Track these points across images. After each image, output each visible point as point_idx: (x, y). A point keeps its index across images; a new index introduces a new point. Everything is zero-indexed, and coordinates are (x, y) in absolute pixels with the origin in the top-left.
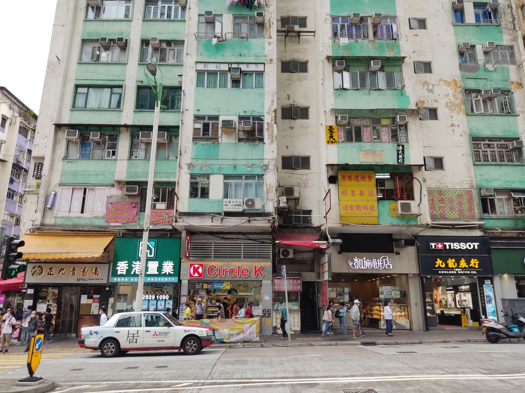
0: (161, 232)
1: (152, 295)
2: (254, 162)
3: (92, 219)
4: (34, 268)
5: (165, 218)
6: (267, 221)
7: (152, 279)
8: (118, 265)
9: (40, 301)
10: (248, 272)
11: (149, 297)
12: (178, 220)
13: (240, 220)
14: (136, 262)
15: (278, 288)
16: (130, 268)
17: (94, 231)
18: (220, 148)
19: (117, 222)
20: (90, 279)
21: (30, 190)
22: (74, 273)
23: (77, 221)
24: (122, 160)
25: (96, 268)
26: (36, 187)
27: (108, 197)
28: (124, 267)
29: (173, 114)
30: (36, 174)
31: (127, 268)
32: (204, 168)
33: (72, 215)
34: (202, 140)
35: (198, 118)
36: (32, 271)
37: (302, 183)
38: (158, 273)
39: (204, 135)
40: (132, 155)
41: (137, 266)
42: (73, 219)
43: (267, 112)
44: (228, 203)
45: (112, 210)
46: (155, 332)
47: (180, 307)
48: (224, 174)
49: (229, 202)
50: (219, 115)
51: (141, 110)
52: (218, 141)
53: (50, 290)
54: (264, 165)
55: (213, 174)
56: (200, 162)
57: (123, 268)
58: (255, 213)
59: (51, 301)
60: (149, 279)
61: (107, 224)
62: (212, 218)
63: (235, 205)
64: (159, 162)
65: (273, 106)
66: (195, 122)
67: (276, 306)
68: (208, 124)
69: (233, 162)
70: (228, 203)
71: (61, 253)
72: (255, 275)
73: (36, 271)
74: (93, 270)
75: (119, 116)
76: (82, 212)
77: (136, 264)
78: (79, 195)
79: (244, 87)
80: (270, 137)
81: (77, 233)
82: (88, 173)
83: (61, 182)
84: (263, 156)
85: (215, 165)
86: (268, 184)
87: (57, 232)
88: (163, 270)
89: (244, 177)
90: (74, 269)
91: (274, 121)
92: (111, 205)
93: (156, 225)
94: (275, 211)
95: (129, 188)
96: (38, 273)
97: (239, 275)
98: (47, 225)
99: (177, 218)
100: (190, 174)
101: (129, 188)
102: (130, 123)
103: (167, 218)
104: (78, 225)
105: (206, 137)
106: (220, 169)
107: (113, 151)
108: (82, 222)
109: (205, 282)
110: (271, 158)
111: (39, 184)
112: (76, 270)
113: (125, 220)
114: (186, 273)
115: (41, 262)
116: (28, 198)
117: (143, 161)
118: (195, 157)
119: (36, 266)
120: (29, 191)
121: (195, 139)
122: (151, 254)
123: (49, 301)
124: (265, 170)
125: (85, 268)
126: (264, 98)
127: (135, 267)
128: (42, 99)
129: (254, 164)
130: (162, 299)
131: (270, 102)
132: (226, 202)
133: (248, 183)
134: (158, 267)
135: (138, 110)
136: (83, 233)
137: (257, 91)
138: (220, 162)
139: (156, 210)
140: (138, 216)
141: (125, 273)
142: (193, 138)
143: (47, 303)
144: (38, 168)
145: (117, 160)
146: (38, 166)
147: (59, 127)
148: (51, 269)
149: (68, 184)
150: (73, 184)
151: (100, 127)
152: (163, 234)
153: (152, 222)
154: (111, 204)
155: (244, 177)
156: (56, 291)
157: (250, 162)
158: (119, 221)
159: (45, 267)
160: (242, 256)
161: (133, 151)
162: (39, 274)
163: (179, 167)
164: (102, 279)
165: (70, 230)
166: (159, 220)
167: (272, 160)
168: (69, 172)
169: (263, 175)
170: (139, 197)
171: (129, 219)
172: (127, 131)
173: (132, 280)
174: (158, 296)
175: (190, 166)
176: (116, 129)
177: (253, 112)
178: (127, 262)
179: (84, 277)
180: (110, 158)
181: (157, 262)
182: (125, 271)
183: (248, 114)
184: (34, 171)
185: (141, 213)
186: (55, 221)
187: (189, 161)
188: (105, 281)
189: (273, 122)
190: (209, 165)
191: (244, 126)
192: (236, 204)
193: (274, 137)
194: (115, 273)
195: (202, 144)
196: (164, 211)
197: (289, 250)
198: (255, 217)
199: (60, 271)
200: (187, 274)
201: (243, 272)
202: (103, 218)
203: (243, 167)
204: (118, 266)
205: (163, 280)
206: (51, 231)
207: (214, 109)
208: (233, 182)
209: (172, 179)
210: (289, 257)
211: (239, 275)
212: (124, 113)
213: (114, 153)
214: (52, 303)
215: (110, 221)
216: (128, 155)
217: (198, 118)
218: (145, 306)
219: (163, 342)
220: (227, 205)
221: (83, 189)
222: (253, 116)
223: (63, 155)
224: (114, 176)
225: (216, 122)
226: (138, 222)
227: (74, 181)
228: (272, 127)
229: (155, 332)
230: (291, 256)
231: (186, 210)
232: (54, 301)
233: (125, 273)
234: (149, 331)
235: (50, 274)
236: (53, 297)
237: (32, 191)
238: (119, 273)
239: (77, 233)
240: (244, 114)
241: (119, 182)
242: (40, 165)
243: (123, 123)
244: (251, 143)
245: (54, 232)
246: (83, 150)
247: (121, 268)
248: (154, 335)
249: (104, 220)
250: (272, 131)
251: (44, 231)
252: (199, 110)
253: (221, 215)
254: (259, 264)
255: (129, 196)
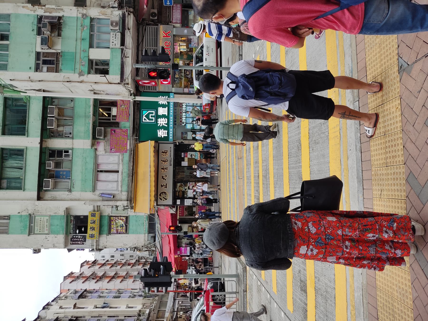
0: (136, 107)
1: (183, 115)
2: (79, 24)
3: (124, 163)
4: (161, 199)
5: (124, 108)
6: (129, 16)
7: (171, 111)
8: (160, 137)
9: (185, 195)
10: (167, 42)
11: (184, 117)
12: (127, 83)
13: (128, 37)
14: (158, 124)
15: (179, 20)
16: (163, 128)
17: (133, 158)
18: (66, 51)
19: (127, 144)
20: (170, 156)
21: (95, 244)
22: (166, 169)
23: (125, 175)
24: (73, 144)
25: (163, 152)
26: (93, 238)
27: (106, 152)
28: (162, 132)
29: (31, 105)
30: (81, 242)
31: (163, 130)
32: (83, 64)
33: (120, 180)
34: (57, 66)
35: (37, 69)
36: (164, 201)
37: (98, 2)
38: (167, 107)
39: (53, 64)
40: (69, 137)
41: (161, 123)
42: (123, 178)
43: (34, 12)
44: (114, 44)
45: (117, 149)
46: (207, 54)
47: (192, 92)
48: (89, 48)
49: (113, 42)
50: (36, 51)
51: (26, 131)
52: (59, 53)
53: (178, 189)
54: (82, 17)
55: (88, 57)
56: (78, 66)
57: (163, 133)
58: (122, 25)
59: (186, 188)
60: (171, 114)
61: (128, 151)
62: (126, 57)
63: (116, 38)
64: (75, 114)
65: (28, 7)
66: (41, 71)
67: (191, 25)
68: (43, 60)
69: (79, 41)
70: (114, 44)
71: (150, 171)
72: (170, 37)
73: (163, 197)
74: (164, 155)
75: (32, 149)
76: (118, 172)
77: (160, 123)
78: (102, 176)
79: (9, 31)
80: (57, 11)
81: (135, 173)
82: (84, 170)
83: (91, 190)
84: (74, 17)
85: (80, 55)
86: (98, 14)
87: (133, 187)
88: (165, 104)
89: (92, 33)
90: (162, 169)
91: (43, 7)
92: (113, 150)
93: (130, 114)
94: (121, 10)
95: (98, 135)
96: (165, 195)
97: (170, 49)
98: (128, 198)
99: (125, 83)
100: (88, 74)
101: (98, 135)
102: (39, 140)
103: (124, 106)
104: (128, 174)
105: (55, 62)
106: (85, 51)
107: (64, 153)
108: (126, 170)
109: (174, 76)
110: (76, 11)
111: (90, 236)
112: (163, 167)
113: (125, 138)
114: (167, 87)
115: (157, 195)
116: (102, 246)
117: (75, 127)
118: (73, 71)
119: (160, 198)
120: (96, 246)
121: (57, 71)
122: (152, 113)
123: (186, 189)
124: (86, 16)
125: (162, 160)
126: (20, 14)
127: (162, 124)
128: (7, 248)
129: (81, 25)
130: (186, 108)
131: (24, 9)
132: (113, 45)
133: (97, 46)
134: (162, 108)
135: (26, 133)
136: (135, 167)
137: (12, 19)
138: (78, 51)
139: (118, 115)
140: (122, 128)
141: (166, 131)
142: (56, 72)
143: (187, 190)
144: (76, 241)
145: (73, 148)
146: (74, 241)
147: (39, 198)
148: (162, 186)
149: (93, 185)
150: (94, 180)
151: (42, 164)
152: (137, 109)
153: (127, 117)
154: (111, 149)
155: (92, 33)
156: (179, 184)
157: (79, 27)
158: (126, 142)
159: (161, 190)
160: (155, 48)
161: (65, 136)
162: (166, 195)
163: (81, 82)
164: (171, 147)
165: (132, 176)
166: (126, 112)
167: (78, 10)
168: (82, 185)
169: (91, 18)
170: (106, 128)
171: (125, 135)
172: (46, 141)
173: (171, 126)
174: (184, 111)
175: (81, 74)
176: (43, 151)
177: (34, 24)
178: (158, 130)
179: (169, 161)
180: (71, 154)
181: (159, 108)
182: (165, 131)
183: (35, 28)
184: (79, 244)
185: (120, 127)
186: (124, 192)
187: (77, 75)
188: (172, 146)
189: (44, 7)
190: (81, 60)
191: (47, 28)
192: (114, 37)
193: (57, 8)
194: (166, 139)
195: (62, 65)
196: (118, 109)
197: (151, 12)
198: (125, 25)
199: (164, 179)
200: (168, 86)
201: (167, 46)
202: (123, 155)
203: (83, 33)
204: (161, 136)
205: (171, 120)
206: (132, 192)
207: (30, 55)
208: (95, 41)
209: (91, 103)
210: (156, 12)
211: (170, 49)
212: (29, 145)
213: (67, 152)
214: (187, 187)
215: (125, 149)
216: (68, 139)
217: (37, 69)
218: (190, 120)
219: (213, 49)
220: (115, 44)
221: (98, 173)
222: (37, 24)
223: (67, 193)
224: (87, 149)
225: (42, 54)
226: (127, 128)
227: (90, 180)
228: (48, 9)
229: (207, 54)
230: (156, 11)
231: (119, 77)
232: (186, 186)
233: (166, 131)
234: (206, 59)
235: (166, 186)
236: (183, 186)
237: (97, 241)
238: (166, 135)
239: (135, 173)
240: (35, 31)
241: (93, 145)
242: (73, 240)
243: (39, 146)
244: (63, 26)
245: (133, 189)
246: (63, 177)
247: (163, 134)
248: (208, 55)
249: (125, 153)
250: (52, 9)
251: (133, 198)
252: (30, 68)
253: (124, 49)
254: (162, 34)
255: (105, 136)
